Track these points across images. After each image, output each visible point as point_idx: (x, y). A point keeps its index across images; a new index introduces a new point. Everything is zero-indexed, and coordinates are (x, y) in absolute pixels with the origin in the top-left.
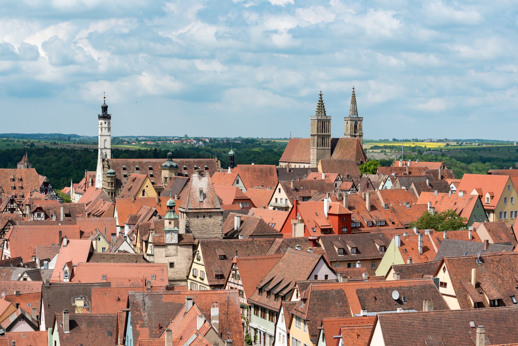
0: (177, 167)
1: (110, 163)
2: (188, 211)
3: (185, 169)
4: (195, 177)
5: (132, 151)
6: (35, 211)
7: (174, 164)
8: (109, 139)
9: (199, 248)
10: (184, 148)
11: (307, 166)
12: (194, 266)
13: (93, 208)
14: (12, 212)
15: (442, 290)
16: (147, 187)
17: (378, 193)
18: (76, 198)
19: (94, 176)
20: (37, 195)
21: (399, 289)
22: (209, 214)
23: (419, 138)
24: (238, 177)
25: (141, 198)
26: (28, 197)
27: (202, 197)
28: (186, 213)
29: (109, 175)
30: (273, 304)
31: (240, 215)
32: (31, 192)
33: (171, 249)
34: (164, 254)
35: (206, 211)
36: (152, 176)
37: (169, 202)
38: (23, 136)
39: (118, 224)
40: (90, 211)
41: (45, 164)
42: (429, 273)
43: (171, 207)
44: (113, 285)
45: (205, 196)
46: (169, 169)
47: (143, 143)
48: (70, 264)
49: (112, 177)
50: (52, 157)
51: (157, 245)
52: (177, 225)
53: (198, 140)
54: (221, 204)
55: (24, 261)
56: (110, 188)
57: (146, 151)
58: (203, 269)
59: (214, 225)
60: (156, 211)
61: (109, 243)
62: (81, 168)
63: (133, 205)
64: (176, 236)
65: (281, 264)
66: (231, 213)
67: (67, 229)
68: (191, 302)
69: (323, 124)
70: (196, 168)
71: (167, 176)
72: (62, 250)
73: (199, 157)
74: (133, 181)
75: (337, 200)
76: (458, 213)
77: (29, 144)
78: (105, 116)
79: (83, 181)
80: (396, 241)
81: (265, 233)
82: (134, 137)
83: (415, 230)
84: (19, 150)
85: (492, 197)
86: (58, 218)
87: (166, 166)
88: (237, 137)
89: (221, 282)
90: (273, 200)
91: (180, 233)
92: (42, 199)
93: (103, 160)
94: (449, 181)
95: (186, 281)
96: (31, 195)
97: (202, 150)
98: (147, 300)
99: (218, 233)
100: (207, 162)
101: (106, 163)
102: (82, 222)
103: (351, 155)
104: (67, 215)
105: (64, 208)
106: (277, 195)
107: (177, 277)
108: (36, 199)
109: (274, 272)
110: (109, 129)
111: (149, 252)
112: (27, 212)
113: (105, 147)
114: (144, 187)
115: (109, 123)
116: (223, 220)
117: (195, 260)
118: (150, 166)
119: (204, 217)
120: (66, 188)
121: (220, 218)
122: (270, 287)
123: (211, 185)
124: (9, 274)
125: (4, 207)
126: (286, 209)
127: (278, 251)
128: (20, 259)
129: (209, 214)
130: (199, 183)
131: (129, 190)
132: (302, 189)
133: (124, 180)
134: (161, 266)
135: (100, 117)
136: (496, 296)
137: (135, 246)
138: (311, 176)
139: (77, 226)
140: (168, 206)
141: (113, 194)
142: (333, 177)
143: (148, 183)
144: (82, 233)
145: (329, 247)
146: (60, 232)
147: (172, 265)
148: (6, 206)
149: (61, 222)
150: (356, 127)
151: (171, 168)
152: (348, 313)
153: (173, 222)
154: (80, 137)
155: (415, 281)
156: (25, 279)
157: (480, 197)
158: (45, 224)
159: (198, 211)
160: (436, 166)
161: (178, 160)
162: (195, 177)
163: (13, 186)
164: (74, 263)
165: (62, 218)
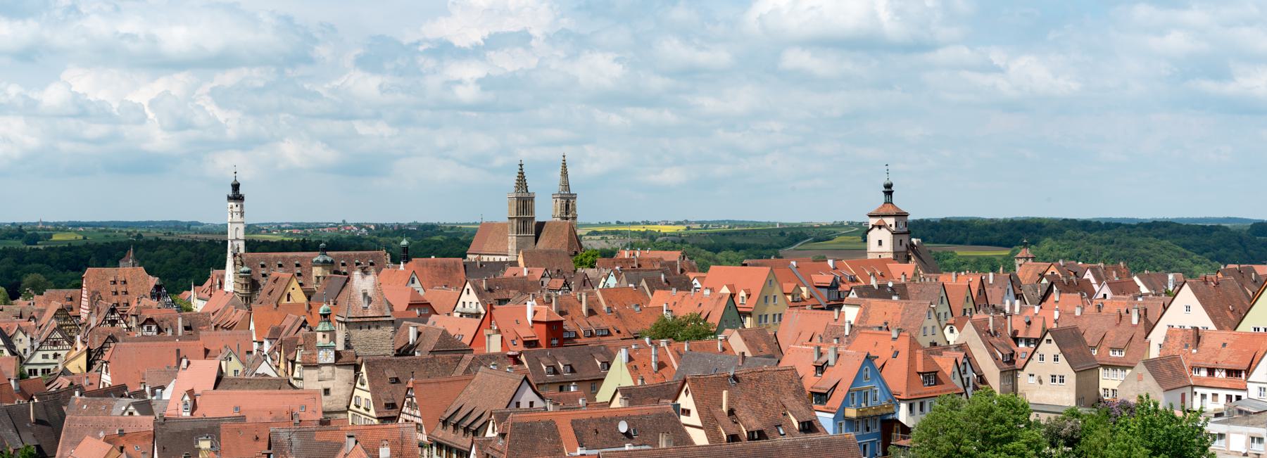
0: (332, 262)
4: (357, 275)
6: (144, 323)
7: (329, 259)
8: (242, 227)
9: (363, 369)
11: (503, 259)
12: (357, 392)
14: (113, 325)
15: (684, 419)
17: (599, 293)
18: (198, 306)
19: (223, 276)
20: (147, 302)
21: (627, 418)
22: (376, 323)
23: (651, 220)
26: (134, 304)
30: (462, 441)
33: (326, 371)
34: (316, 378)
36: (299, 275)
37: (323, 309)
41: (157, 262)
42: (667, 397)
43: (325, 316)
44: (249, 419)
45: (370, 301)
48: (191, 393)
50: (165, 251)
51: (306, 366)
52: (333, 338)
53: (360, 226)
54: (392, 310)
55: (130, 390)
57: (291, 243)
58: (368, 396)
59: (383, 338)
61: (244, 364)
63: (275, 313)
64: (332, 353)
65: (471, 387)
67: (188, 346)
68: (353, 440)
69: (525, 203)
72: (181, 374)
74: (275, 281)
75: (545, 303)
76: (703, 317)
78: (237, 197)
80: (622, 356)
81: (449, 348)
83: (647, 340)
85: (749, 296)
89: (393, 413)
90: (460, 305)
91: (338, 349)
92: (153, 307)
93: (235, 255)
94: (691, 275)
95: (346, 412)
98: (294, 439)
99: (388, 349)
102: (207, 337)
103: (561, 244)
104: (187, 328)
106: (464, 297)
107: (333, 407)
108: (145, 307)
109: (462, 399)
110: (242, 214)
111: (297, 375)
113: (236, 237)
114: (290, 290)
115: (242, 206)
116: (395, 332)
117: (358, 385)
121: (391, 329)
122: (458, 418)
123: (378, 286)
124: (110, 407)
126: (477, 315)
127: (467, 371)
128: (124, 387)
130: (362, 283)
132: (498, 289)
133: (262, 281)
134: (313, 393)
135: (230, 199)
136: (756, 425)
137: (278, 367)
138: (509, 272)
139: (200, 342)
141: (248, 299)
142: (538, 273)
143: (295, 284)
144: (207, 351)
145: (535, 365)
146: (178, 351)
147: (327, 391)
150: (567, 206)
151: (325, 264)
152: (562, 451)
153: (328, 335)
155: (648, 408)
156: (131, 414)
157: (732, 296)
160: (674, 256)
161: (335, 253)
162: (357, 275)
164: (197, 391)
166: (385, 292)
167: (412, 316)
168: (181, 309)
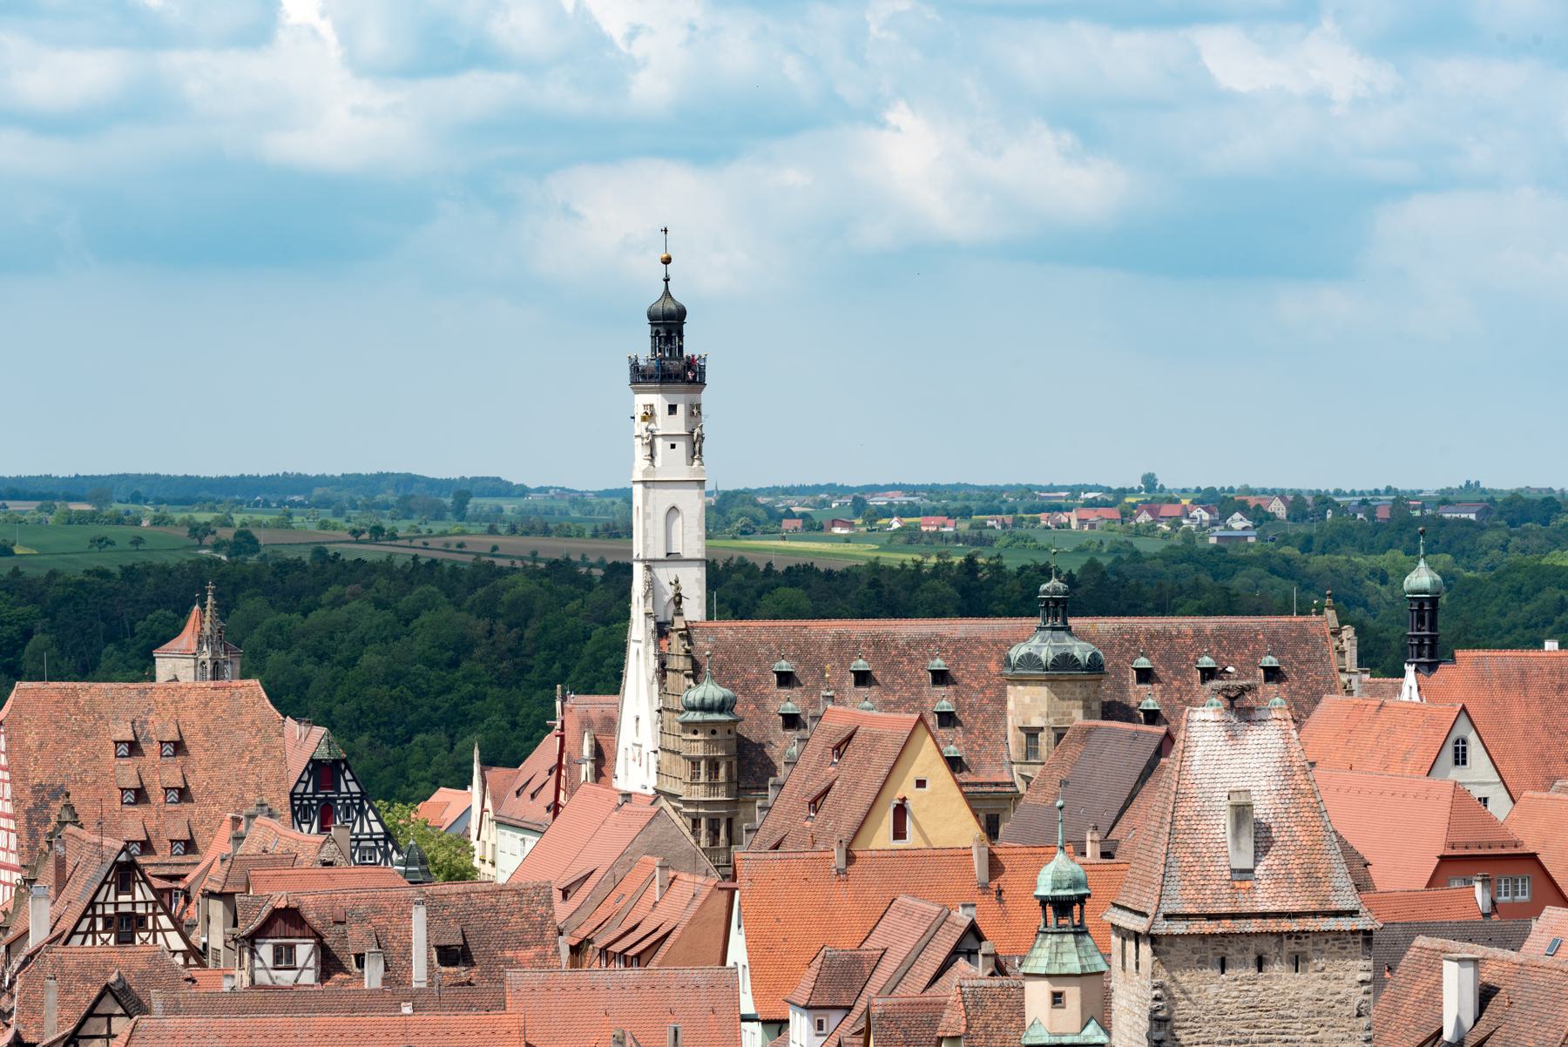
0: (1095, 666)
1: (703, 645)
2: (1163, 927)
3: (1145, 676)
4: (1204, 722)
5: (829, 574)
6: (261, 932)
7: (1080, 651)
8: (693, 505)
10: (1136, 554)
13: (603, 912)
14: (125, 939)
16: (921, 783)
18: (502, 856)
19: (610, 724)
22: (1289, 943)
24: (1463, 719)
25: (885, 855)
26: (217, 846)
27: (1248, 844)
28: (1154, 939)
29: (698, 716)
31: (1479, 951)
32: (236, 821)
35: (1272, 925)
36: (947, 719)
37: (1053, 873)
38: (189, 491)
39: (747, 1007)
40: (583, 932)
41: (321, 657)
43: (1062, 906)
46: (1050, 681)
47: (896, 524)
49: (712, 727)
50: (361, 613)
53: (1221, 503)
54: (1362, 885)
56: (699, 794)
57: (914, 576)
59: (1321, 1011)
60: (973, 931)
62: (533, 676)
66: (1421, 941)
70: (1208, 674)
71: (1036, 722)
73: (1230, 606)
74: (841, 748)
77: (227, 534)
78: (671, 365)
79: (546, 752)
82: (843, 490)
84: (166, 572)
86: (395, 975)
87: (1030, 660)
88: (1456, 483)
92: (301, 862)
93: (662, 630)
96: (238, 839)
97: (1248, 562)
100: (1273, 637)
101: (676, 644)
104: (449, 955)
105: (431, 913)
112: (216, 937)
113: (668, 548)
115: (694, 411)
116: (1376, 984)
118: (939, 664)
119: (1260, 963)
120: (443, 794)
123: (1299, 775)
125: (80, 907)
129: (1290, 946)
131: (815, 803)
133: (783, 745)
135: (641, 377)
139: (506, 1020)
140: (1044, 902)
143: (927, 760)
148: (92, 904)
149: (416, 998)
153: (1073, 994)
154: (523, 491)
158: (322, 1010)
159: (1226, 926)
161: (1105, 625)
162: (1204, 722)
163: (135, 784)
165: (419, 972)
166: (1331, 802)
167: (1456, 915)
168: (422, 868)
